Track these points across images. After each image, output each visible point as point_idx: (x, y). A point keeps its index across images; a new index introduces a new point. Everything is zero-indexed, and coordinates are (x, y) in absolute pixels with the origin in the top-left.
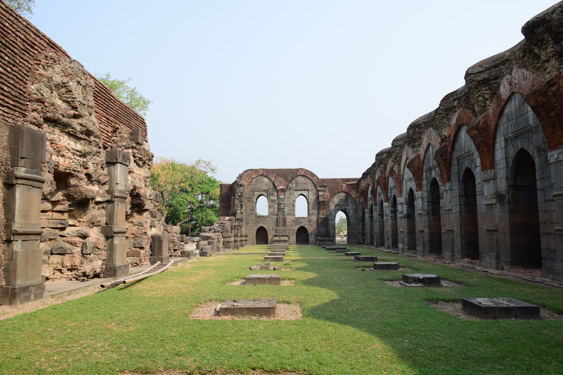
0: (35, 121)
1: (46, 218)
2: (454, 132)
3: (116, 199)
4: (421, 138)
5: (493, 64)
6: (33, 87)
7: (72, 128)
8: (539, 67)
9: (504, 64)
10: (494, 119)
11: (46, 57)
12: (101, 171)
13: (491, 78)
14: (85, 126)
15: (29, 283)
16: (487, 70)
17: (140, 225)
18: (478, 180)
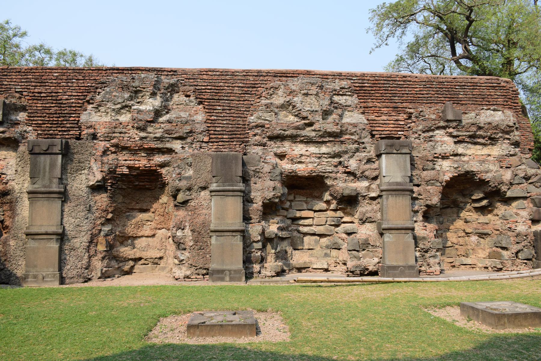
0: (257, 143)
1: (324, 216)
3: (384, 193)
6: (252, 118)
7: (303, 137)
11: (267, 88)
12: (368, 166)
14: (319, 131)
15: (225, 267)
17: (504, 218)
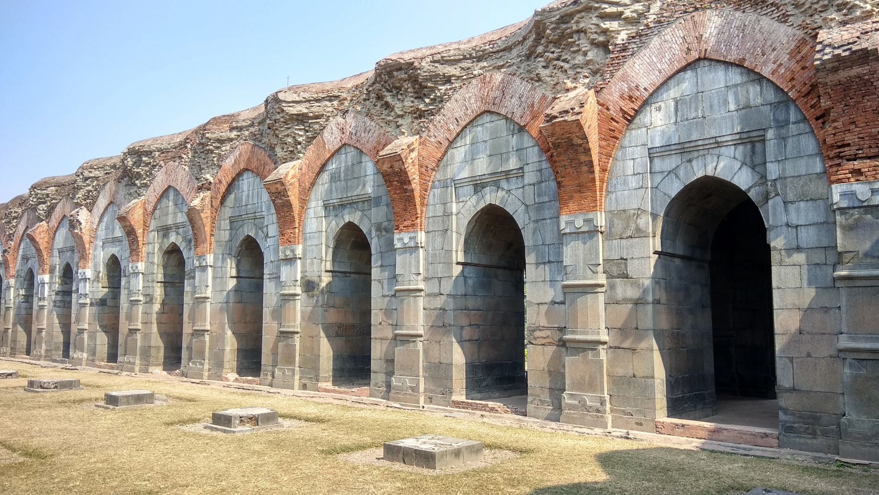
2: (229, 179)
4: (151, 174)
5: (315, 96)
8: (390, 121)
9: (330, 101)
10: (311, 174)
13: (311, 115)
16: (305, 102)
18: (268, 257)
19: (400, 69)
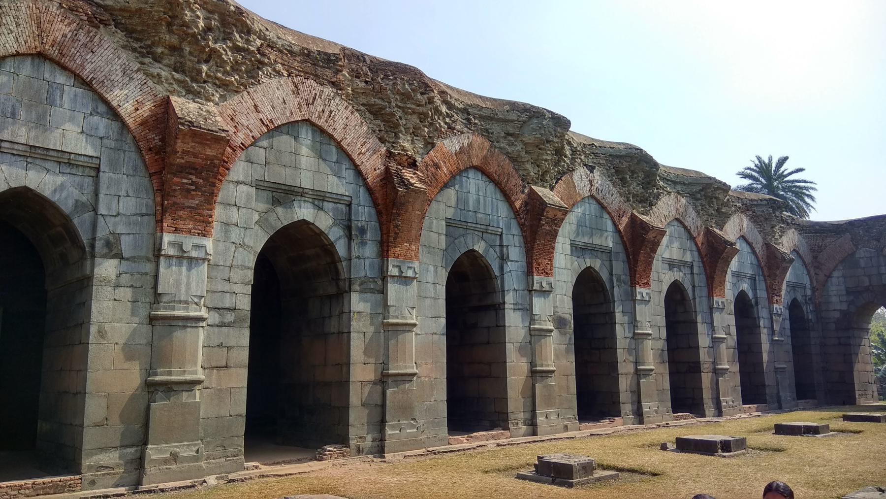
19: (647, 163)
